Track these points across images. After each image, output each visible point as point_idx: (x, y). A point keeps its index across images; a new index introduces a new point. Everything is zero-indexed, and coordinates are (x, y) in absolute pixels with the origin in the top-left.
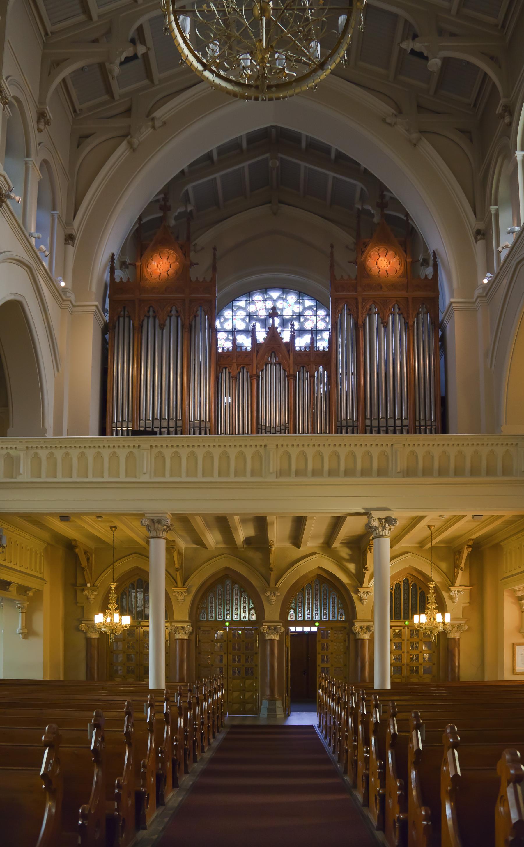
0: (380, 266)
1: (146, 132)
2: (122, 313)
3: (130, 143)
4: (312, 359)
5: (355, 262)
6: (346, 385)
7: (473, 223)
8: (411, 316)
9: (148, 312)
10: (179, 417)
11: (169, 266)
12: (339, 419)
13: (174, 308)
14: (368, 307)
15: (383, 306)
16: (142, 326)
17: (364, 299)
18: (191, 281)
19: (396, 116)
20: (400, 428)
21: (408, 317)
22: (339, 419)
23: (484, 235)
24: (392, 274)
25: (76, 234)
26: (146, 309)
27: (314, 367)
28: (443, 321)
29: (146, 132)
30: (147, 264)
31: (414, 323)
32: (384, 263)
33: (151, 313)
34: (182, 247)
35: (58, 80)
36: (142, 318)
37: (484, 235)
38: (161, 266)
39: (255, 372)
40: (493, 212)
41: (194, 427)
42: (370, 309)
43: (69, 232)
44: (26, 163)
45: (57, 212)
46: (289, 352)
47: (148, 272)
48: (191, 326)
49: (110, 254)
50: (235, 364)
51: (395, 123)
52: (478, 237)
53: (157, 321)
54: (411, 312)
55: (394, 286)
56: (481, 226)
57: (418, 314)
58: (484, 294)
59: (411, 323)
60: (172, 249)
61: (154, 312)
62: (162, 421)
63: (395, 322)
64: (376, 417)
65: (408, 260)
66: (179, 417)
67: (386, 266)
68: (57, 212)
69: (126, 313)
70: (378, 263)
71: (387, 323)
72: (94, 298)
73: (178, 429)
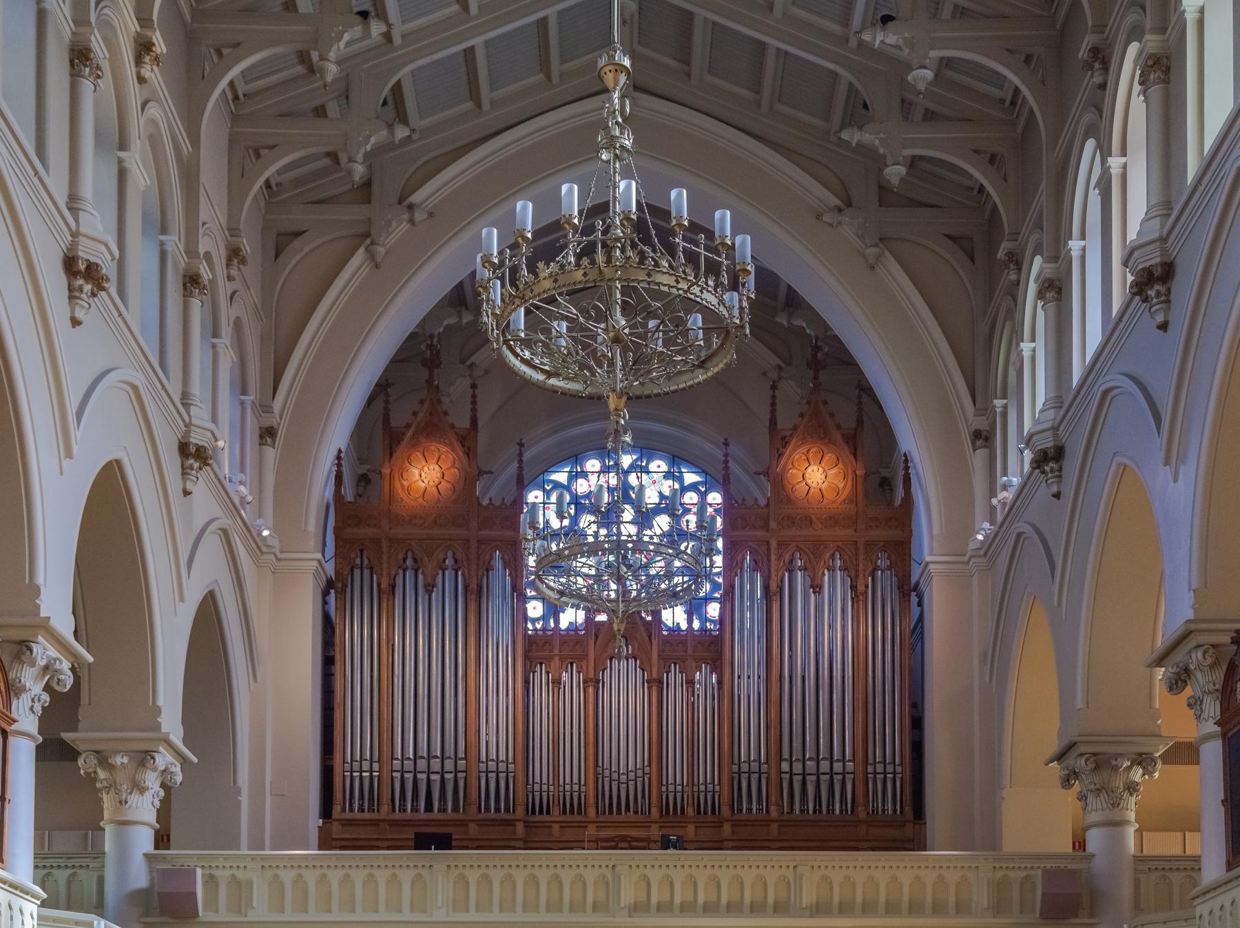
0: (809, 482)
1: (400, 228)
2: (358, 561)
3: (371, 256)
4: (690, 651)
5: (766, 474)
6: (749, 685)
7: (969, 418)
8: (861, 576)
9: (405, 560)
10: (461, 754)
11: (439, 475)
12: (736, 761)
13: (450, 554)
14: (787, 557)
15: (815, 552)
16: (393, 587)
17: (780, 545)
18: (480, 504)
19: (840, 210)
20: (840, 777)
21: (857, 576)
22: (736, 761)
23: (987, 439)
24: (830, 496)
25: (279, 425)
26: (401, 556)
27: (694, 664)
28: (917, 584)
29: (400, 228)
30: (402, 471)
31: (867, 587)
32: (817, 476)
33: (409, 562)
34: (462, 440)
35: (261, 182)
36: (393, 572)
37: (987, 439)
38: (425, 475)
39: (591, 675)
40: (998, 410)
41: (487, 772)
42: (791, 561)
43: (267, 423)
44: (214, 346)
45: (252, 398)
46: (650, 637)
47: (403, 486)
48: (480, 588)
49: (335, 452)
50: (557, 659)
51: (840, 223)
52: (979, 443)
53: (420, 577)
54: (861, 567)
55: (833, 520)
56: (982, 424)
57: (875, 569)
58: (982, 552)
59: (861, 588)
60: (445, 444)
61: (415, 561)
62: (432, 761)
63: (835, 585)
64: (800, 757)
65: (858, 473)
66: (461, 754)
67: (820, 482)
68: (252, 398)
69: (366, 562)
70: (807, 476)
71: (821, 587)
72: (312, 543)
73: (459, 775)
